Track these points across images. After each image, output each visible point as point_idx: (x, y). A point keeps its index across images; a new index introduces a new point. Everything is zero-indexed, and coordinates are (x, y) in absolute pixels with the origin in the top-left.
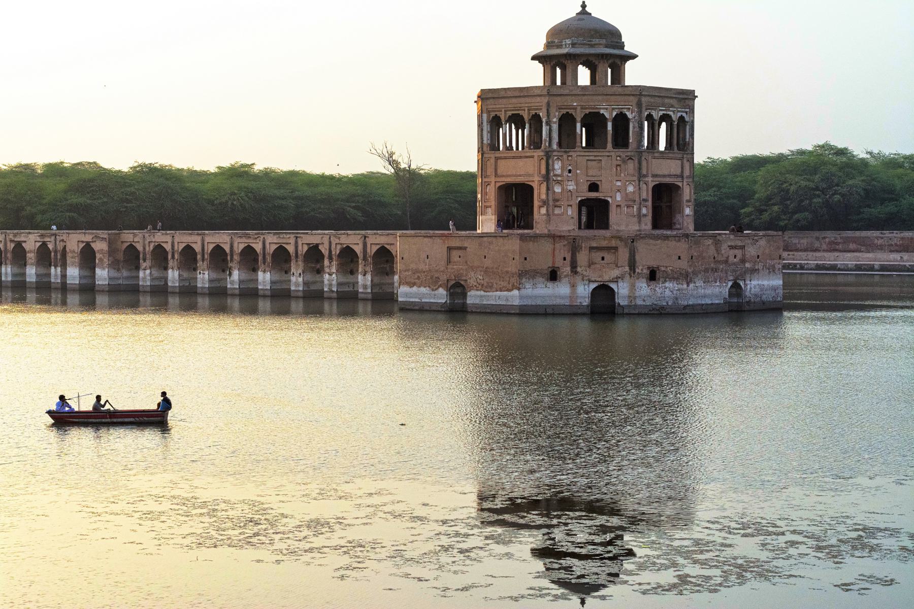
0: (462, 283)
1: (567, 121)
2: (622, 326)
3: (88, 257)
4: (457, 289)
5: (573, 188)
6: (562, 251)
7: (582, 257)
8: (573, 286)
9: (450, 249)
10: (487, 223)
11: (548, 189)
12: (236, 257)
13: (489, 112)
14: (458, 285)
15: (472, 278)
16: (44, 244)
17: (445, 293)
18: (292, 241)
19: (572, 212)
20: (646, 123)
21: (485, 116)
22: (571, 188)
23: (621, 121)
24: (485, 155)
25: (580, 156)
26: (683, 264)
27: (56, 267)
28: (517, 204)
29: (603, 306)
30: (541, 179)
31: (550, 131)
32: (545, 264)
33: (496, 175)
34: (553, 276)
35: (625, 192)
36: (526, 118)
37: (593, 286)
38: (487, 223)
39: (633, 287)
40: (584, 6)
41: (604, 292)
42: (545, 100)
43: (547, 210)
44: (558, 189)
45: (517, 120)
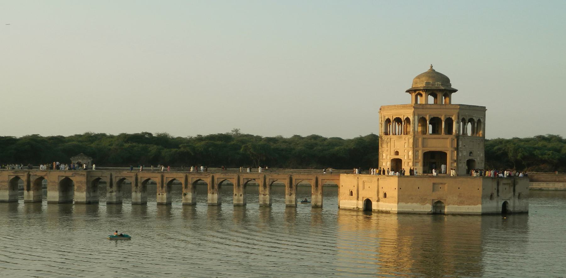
0: (442, 201)
3: (66, 186)
4: (438, 205)
8: (498, 202)
9: (434, 184)
11: (458, 154)
12: (190, 186)
13: (418, 115)
14: (439, 202)
16: (17, 178)
17: (431, 206)
18: (235, 176)
19: (464, 167)
20: (462, 123)
21: (416, 117)
22: (465, 154)
24: (416, 137)
27: (28, 190)
30: (453, 149)
33: (423, 147)
34: (491, 197)
35: (479, 157)
36: (443, 118)
37: (503, 202)
39: (514, 202)
40: (432, 67)
41: (505, 205)
42: (458, 111)
43: (457, 164)
44: (460, 155)
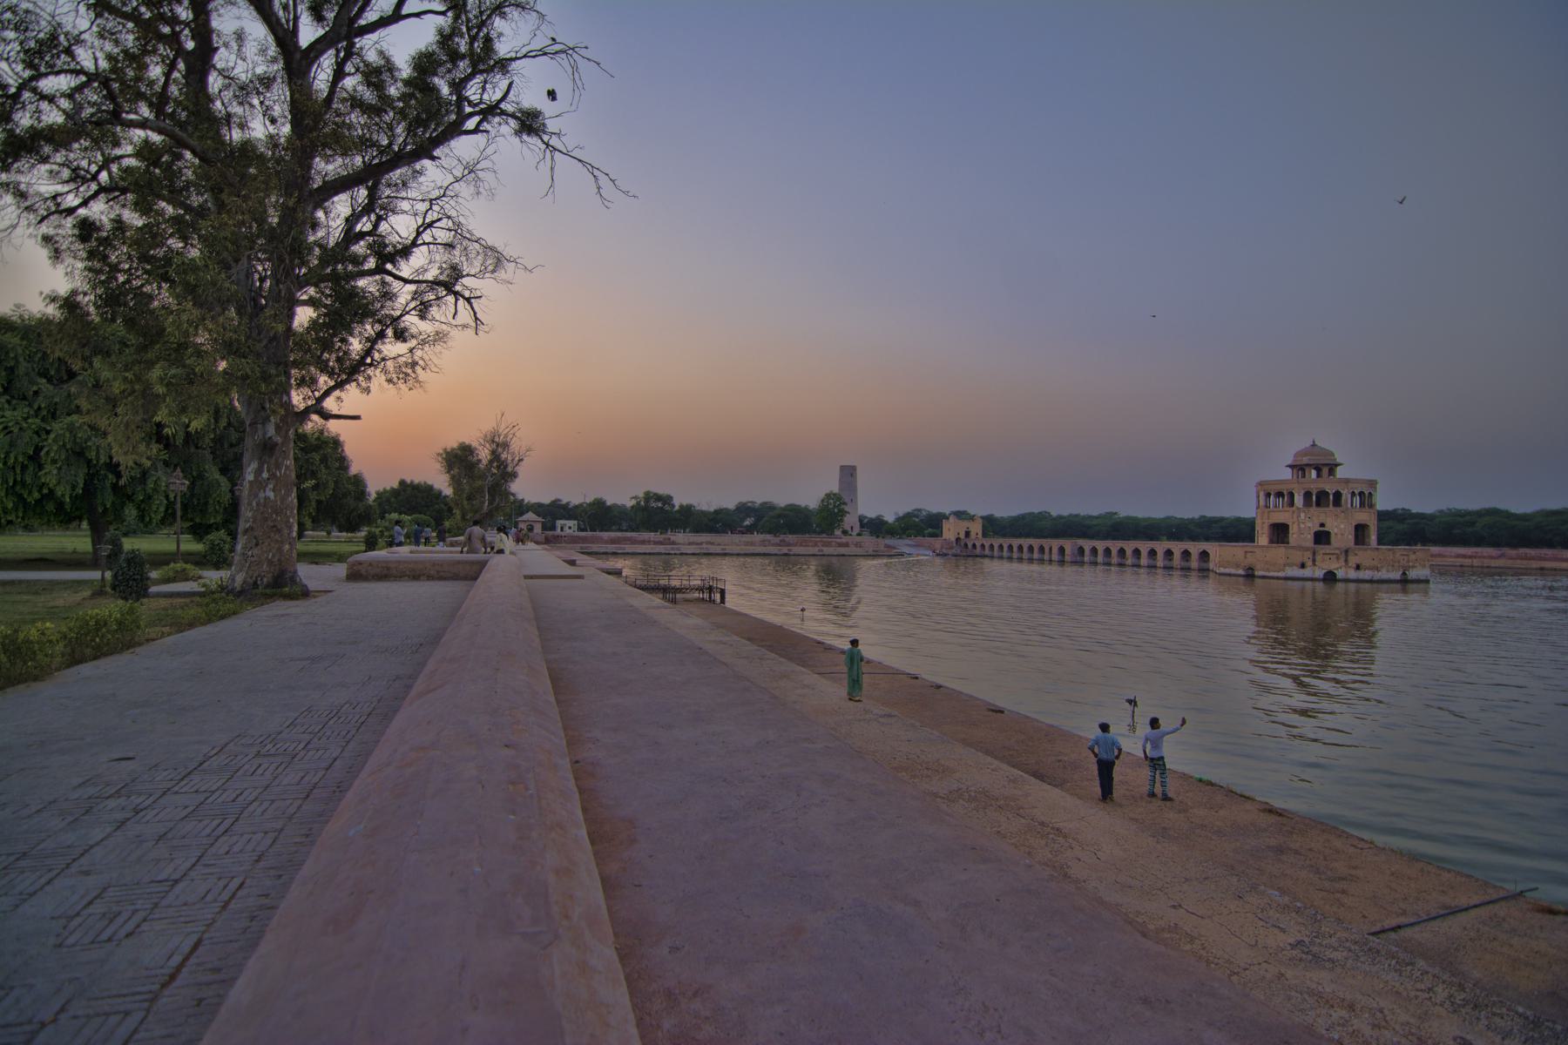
1: (1308, 495)
2: (1340, 587)
6: (1309, 554)
7: (1318, 558)
10: (1263, 539)
19: (1310, 537)
23: (1338, 495)
25: (1314, 509)
26: (1375, 563)
28: (1280, 533)
29: (1330, 578)
31: (1299, 500)
32: (1299, 560)
34: (1303, 566)
38: (1263, 539)
45: (1280, 494)
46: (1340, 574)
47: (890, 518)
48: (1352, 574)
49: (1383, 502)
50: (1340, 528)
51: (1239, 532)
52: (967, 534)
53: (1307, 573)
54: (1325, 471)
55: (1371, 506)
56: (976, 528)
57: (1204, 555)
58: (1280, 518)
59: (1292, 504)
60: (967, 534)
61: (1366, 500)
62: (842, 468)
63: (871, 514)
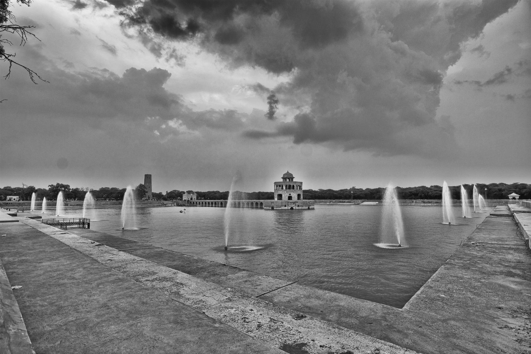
1: (286, 186)
5: (288, 195)
10: (276, 199)
15: (275, 206)
19: (287, 198)
23: (293, 186)
28: (280, 197)
31: (284, 188)
32: (284, 204)
34: (285, 206)
38: (276, 199)
46: (294, 208)
47: (164, 194)
48: (297, 208)
49: (304, 188)
50: (294, 196)
51: (270, 196)
52: (191, 199)
53: (286, 208)
54: (291, 180)
55: (301, 189)
56: (195, 197)
57: (261, 204)
58: (280, 193)
59: (282, 188)
60: (191, 199)
61: (300, 187)
62: (146, 176)
63: (158, 192)
